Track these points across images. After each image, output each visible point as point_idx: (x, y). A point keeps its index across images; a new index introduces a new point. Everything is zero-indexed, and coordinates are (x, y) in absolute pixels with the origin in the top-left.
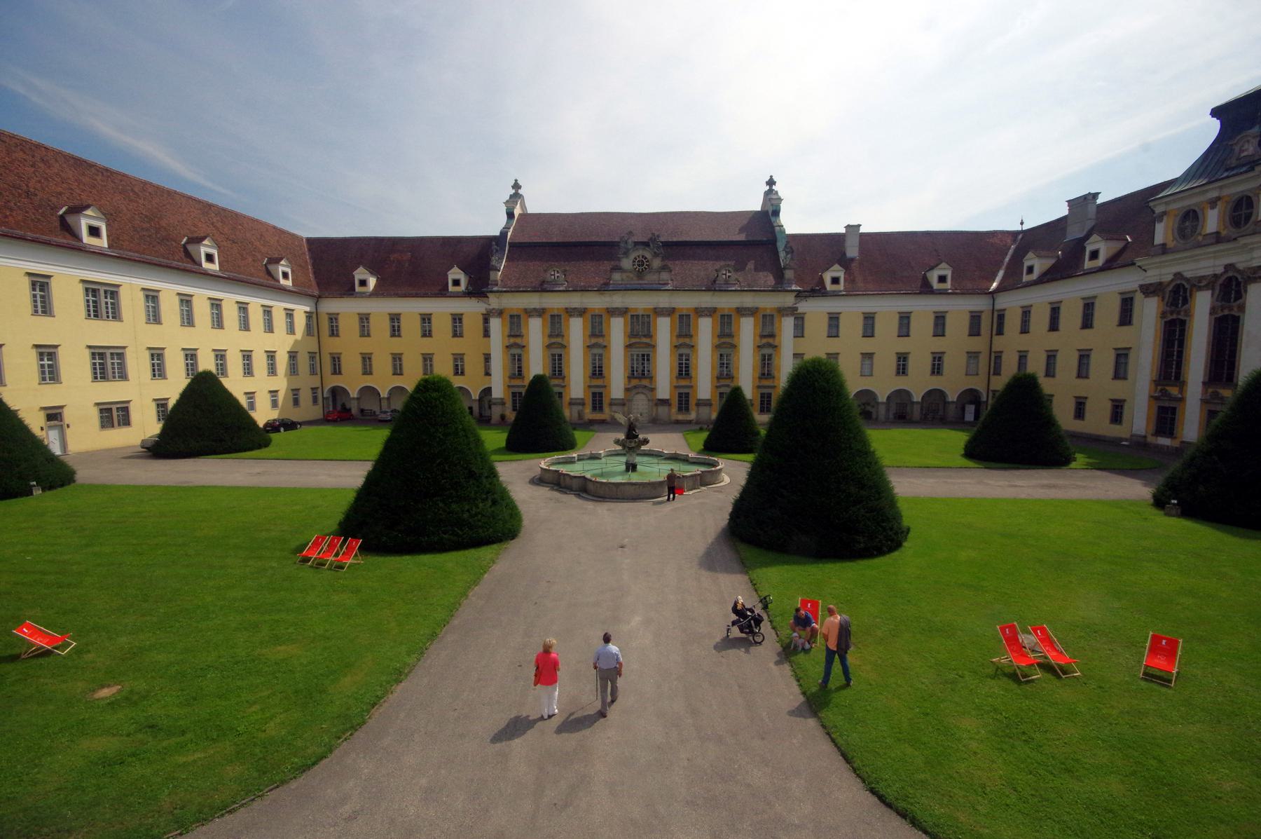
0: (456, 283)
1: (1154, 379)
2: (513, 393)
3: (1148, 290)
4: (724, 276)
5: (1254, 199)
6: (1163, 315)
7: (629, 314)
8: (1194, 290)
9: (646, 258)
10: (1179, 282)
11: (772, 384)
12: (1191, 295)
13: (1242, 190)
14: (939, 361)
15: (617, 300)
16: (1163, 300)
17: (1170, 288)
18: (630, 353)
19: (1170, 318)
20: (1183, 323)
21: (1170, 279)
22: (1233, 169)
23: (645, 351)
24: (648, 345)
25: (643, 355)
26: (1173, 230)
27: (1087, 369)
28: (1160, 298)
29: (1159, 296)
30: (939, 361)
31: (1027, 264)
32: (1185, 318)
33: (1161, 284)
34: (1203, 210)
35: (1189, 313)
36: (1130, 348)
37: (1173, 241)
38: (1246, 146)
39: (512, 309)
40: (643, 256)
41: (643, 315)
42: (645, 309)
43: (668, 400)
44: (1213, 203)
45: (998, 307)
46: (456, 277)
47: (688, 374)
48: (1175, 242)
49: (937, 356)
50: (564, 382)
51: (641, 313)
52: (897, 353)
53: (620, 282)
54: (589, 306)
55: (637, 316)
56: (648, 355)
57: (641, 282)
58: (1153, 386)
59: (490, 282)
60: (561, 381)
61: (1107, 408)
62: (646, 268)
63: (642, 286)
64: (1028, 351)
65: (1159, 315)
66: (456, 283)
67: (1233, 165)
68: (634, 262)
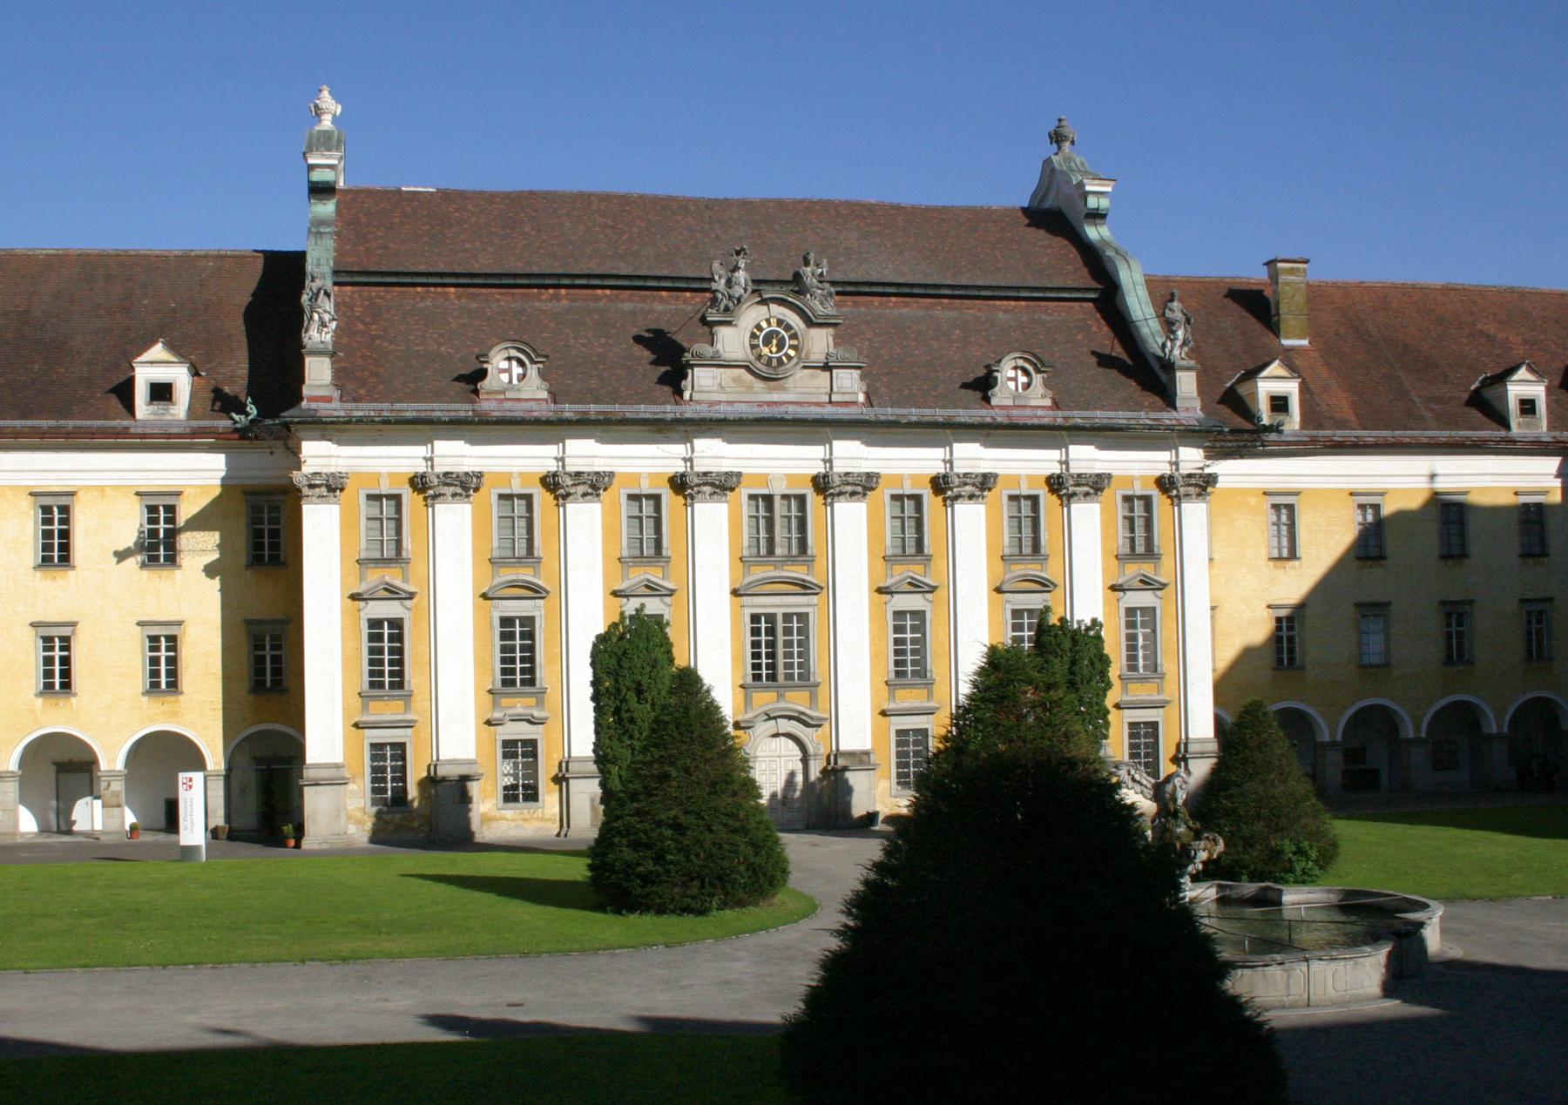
0: (161, 392)
2: (373, 746)
4: (1012, 385)
7: (744, 492)
9: (788, 328)
11: (1155, 697)
14: (1539, 621)
15: (713, 454)
18: (748, 612)
23: (796, 603)
24: (805, 587)
25: (787, 617)
30: (1539, 621)
39: (376, 477)
40: (780, 322)
41: (785, 497)
42: (791, 478)
43: (867, 753)
46: (161, 374)
47: (921, 672)
49: (1535, 607)
50: (540, 703)
51: (778, 489)
52: (1443, 603)
53: (717, 397)
54: (619, 467)
55: (768, 499)
56: (803, 618)
57: (776, 397)
59: (306, 391)
60: (532, 701)
62: (789, 358)
63: (791, 408)
66: (161, 392)
68: (753, 336)
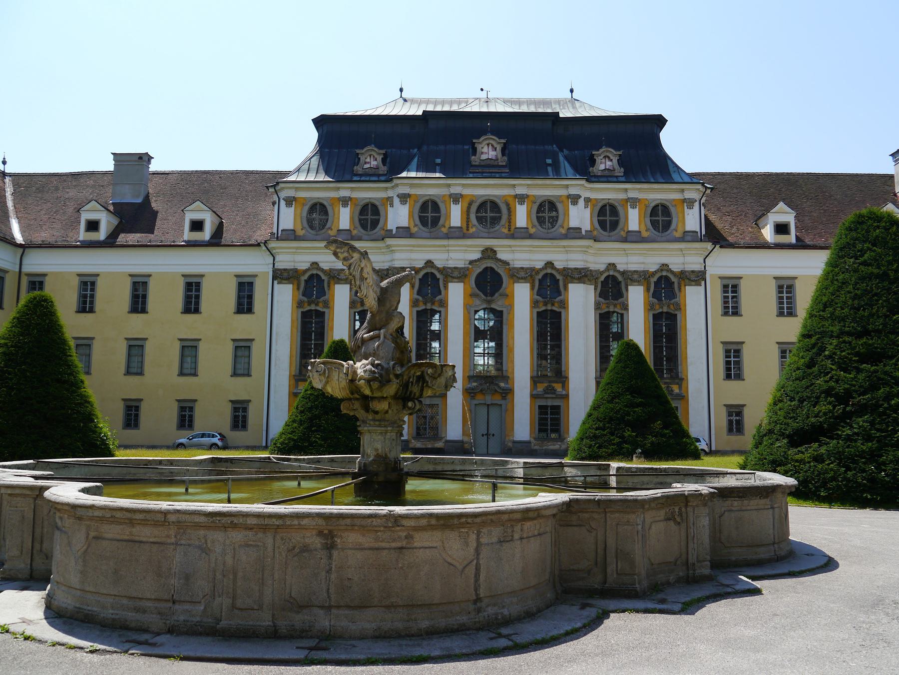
1: (293, 373)
3: (280, 276)
5: (381, 209)
6: (300, 304)
8: (332, 282)
10: (315, 272)
12: (329, 286)
13: (369, 197)
16: (298, 289)
17: (306, 277)
19: (307, 308)
20: (321, 315)
21: (304, 268)
22: (361, 175)
26: (301, 218)
27: (195, 362)
28: (296, 287)
29: (293, 284)
31: (85, 216)
32: (324, 310)
33: (296, 270)
34: (332, 205)
35: (328, 304)
36: (253, 340)
37: (302, 229)
38: (368, 160)
44: (345, 201)
45: (26, 269)
48: (304, 231)
58: (293, 382)
61: (172, 414)
64: (93, 338)
65: (295, 306)
67: (360, 173)
